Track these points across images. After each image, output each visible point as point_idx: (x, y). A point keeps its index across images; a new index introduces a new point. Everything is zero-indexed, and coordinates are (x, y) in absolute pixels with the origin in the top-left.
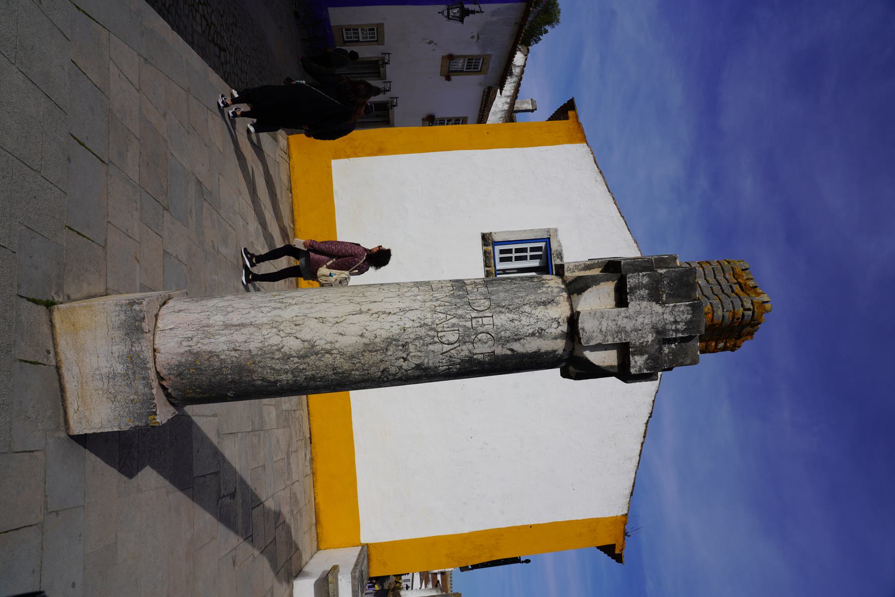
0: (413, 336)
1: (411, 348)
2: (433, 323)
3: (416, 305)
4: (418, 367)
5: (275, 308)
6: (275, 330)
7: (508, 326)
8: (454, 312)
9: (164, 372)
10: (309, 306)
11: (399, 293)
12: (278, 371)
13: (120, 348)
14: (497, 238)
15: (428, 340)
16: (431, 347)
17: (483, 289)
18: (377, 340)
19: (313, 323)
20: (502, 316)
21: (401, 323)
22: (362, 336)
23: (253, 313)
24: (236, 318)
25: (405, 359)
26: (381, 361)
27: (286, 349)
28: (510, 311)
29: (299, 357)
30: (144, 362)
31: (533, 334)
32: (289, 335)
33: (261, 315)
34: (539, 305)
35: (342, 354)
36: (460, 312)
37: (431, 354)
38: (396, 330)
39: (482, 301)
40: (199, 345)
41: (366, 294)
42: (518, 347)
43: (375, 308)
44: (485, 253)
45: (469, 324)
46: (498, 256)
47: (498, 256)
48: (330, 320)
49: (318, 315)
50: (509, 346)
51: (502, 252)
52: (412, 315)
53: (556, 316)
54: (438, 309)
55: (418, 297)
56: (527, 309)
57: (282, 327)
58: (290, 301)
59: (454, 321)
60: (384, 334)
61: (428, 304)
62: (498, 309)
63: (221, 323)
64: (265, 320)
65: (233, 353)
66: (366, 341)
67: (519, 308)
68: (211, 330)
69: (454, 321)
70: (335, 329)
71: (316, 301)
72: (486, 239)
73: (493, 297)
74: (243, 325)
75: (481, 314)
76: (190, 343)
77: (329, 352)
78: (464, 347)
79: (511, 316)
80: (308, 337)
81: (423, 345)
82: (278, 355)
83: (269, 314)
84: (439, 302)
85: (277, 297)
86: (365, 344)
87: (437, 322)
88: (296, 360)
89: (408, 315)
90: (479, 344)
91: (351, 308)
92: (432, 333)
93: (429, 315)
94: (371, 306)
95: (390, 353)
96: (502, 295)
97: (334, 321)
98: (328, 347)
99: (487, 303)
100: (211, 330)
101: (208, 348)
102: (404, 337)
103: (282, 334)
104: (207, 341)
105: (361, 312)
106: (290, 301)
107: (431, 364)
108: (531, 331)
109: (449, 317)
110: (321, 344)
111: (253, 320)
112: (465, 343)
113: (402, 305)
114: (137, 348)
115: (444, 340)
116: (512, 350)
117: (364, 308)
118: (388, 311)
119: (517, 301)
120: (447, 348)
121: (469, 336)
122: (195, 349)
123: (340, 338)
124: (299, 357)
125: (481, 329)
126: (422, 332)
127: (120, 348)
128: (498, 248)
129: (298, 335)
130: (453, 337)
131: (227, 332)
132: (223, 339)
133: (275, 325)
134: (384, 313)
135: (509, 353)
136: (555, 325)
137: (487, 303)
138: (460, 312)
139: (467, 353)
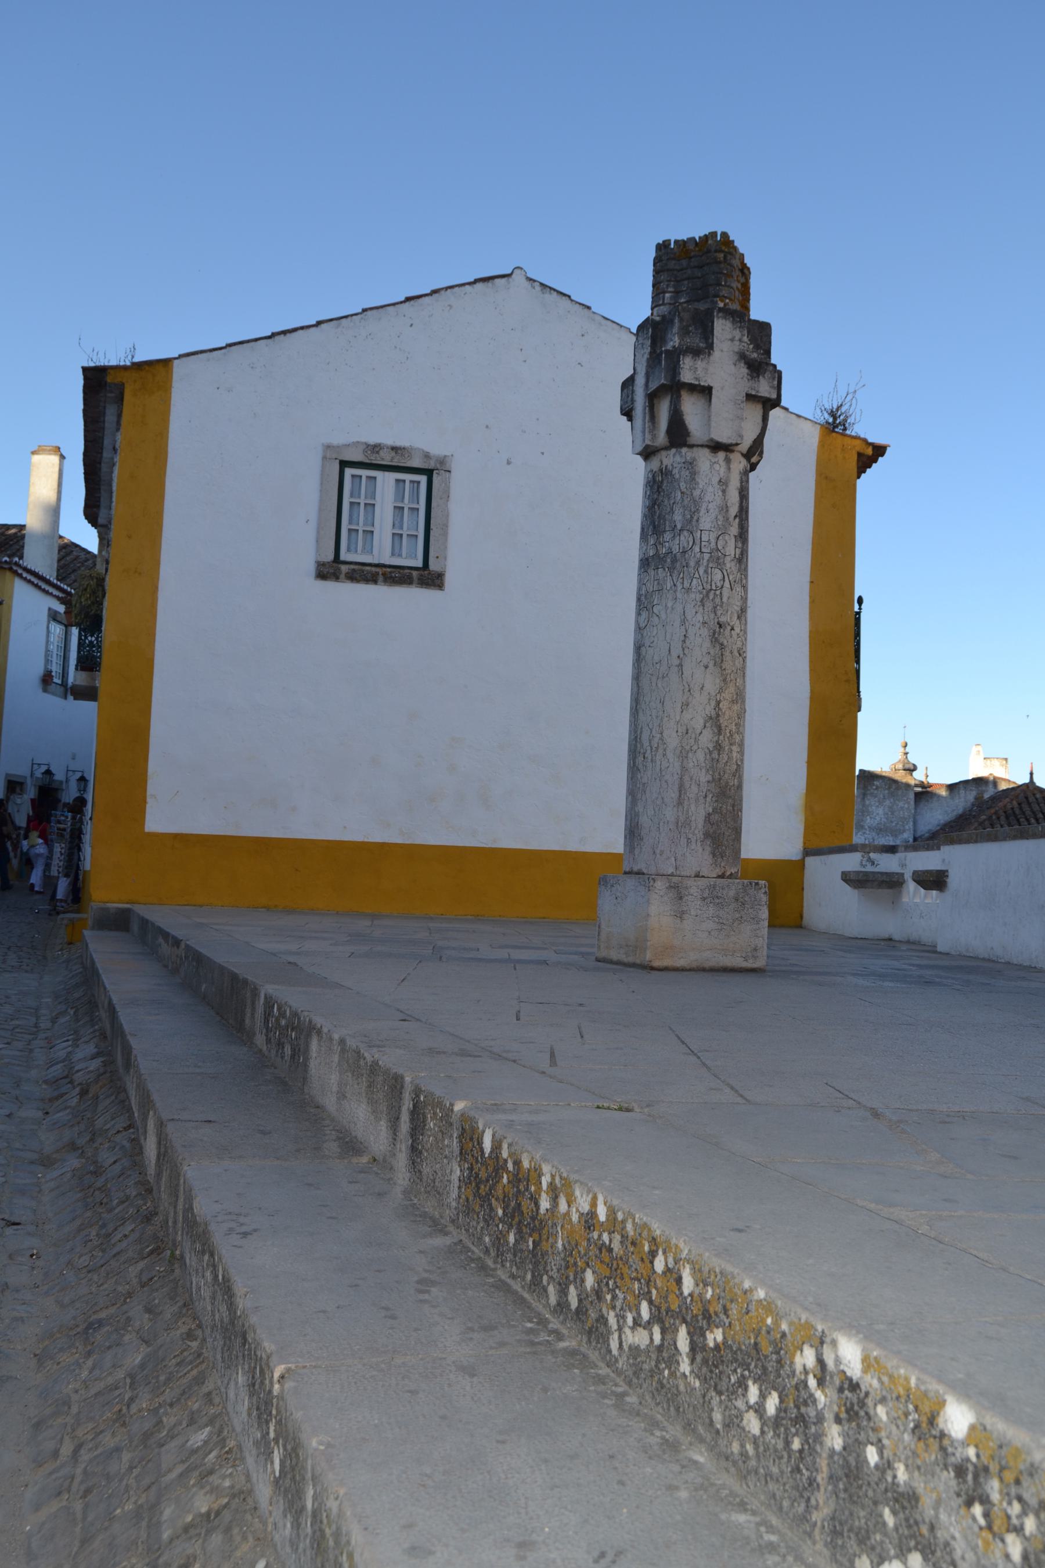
0: (712, 616)
1: (722, 619)
2: (701, 593)
3: (679, 608)
4: (739, 617)
5: (664, 755)
6: (690, 755)
7: (713, 516)
8: (692, 570)
9: (719, 871)
10: (666, 719)
11: (660, 627)
14: (330, 556)
15: (717, 600)
16: (725, 599)
17: (667, 536)
18: (712, 653)
19: (687, 716)
20: (702, 520)
21: (698, 625)
22: (706, 667)
23: (667, 777)
24: (672, 794)
25: (732, 629)
26: (731, 652)
27: (711, 746)
28: (698, 511)
29: (720, 733)
31: (724, 491)
32: (696, 740)
33: (670, 769)
34: (694, 479)
35: (721, 691)
36: (692, 564)
37: (731, 600)
38: (705, 632)
39: (682, 538)
40: (696, 832)
41: (656, 659)
42: (734, 510)
43: (676, 651)
44: (352, 577)
45: (707, 556)
48: (685, 697)
49: (679, 710)
50: (731, 519)
52: (690, 613)
53: (708, 463)
54: (686, 585)
55: (670, 604)
56: (697, 493)
57: (688, 748)
58: (656, 740)
59: (701, 570)
60: (707, 644)
61: (679, 595)
62: (694, 523)
63: (675, 809)
64: (677, 764)
65: (708, 799)
66: (711, 665)
67: (695, 501)
68: (682, 819)
69: (701, 570)
71: (661, 713)
72: (329, 571)
73: (679, 527)
74: (681, 788)
75: (698, 542)
76: (693, 840)
77: (718, 703)
78: (728, 565)
79: (703, 511)
80: (702, 722)
81: (721, 606)
82: (715, 755)
83: (671, 760)
84: (678, 584)
85: (648, 755)
86: (715, 665)
87: (700, 588)
88: (721, 737)
89: (689, 617)
90: (727, 549)
91: (674, 676)
92: (711, 596)
93: (693, 596)
94: (674, 654)
95: (725, 643)
97: (687, 694)
98: (713, 703)
99: (685, 533)
100: (682, 819)
102: (713, 624)
103: (695, 748)
104: (693, 824)
105: (681, 665)
106: (656, 740)
107: (739, 604)
108: (720, 493)
109: (697, 575)
110: (710, 710)
111: (676, 777)
112: (724, 564)
113: (677, 623)
115: (719, 584)
116: (736, 517)
117: (677, 662)
118: (682, 638)
119: (686, 502)
120: (727, 584)
121: (718, 558)
122: (700, 835)
124: (720, 732)
126: (709, 605)
128: (344, 556)
129: (698, 732)
130: (718, 576)
131: (686, 803)
132: (693, 807)
133: (683, 755)
134: (684, 641)
135: (737, 520)
136: (717, 467)
137: (685, 533)
138: (692, 564)
139: (733, 564)
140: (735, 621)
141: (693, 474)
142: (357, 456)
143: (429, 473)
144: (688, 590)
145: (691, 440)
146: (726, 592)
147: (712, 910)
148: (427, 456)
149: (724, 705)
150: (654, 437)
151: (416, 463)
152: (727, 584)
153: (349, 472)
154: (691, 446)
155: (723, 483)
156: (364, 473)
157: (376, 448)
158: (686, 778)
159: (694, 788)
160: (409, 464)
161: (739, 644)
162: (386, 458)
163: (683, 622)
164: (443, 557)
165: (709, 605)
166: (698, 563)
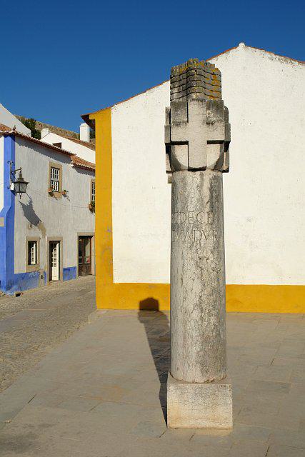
15: (198, 246)
16: (202, 245)
19: (185, 304)
25: (208, 259)
27: (197, 318)
31: (200, 191)
35: (202, 291)
36: (185, 229)
42: (206, 200)
45: (192, 225)
52: (185, 253)
53: (191, 178)
60: (194, 268)
70: (189, 293)
82: (200, 323)
88: (203, 314)
98: (198, 298)
101: (194, 355)
102: (196, 258)
110: (196, 300)
123: (194, 291)
125: (195, 218)
130: (198, 234)
136: (196, 179)
144: (184, 242)
146: (203, 241)
147: (201, 400)
155: (200, 187)
165: (194, 249)
166: (188, 229)
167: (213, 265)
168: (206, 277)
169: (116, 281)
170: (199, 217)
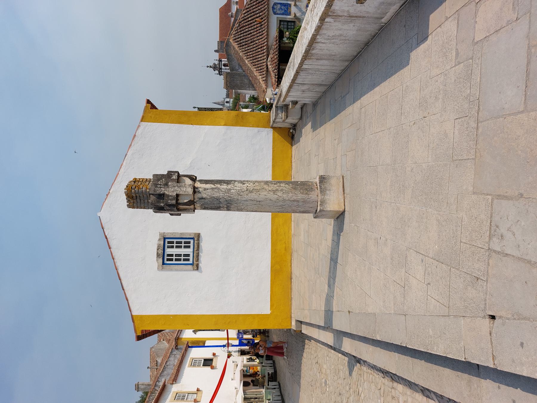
1: (245, 189)
3: (243, 202)
4: (244, 184)
9: (316, 190)
12: (285, 187)
13: (327, 197)
14: (190, 267)
17: (221, 205)
30: (321, 193)
38: (250, 195)
42: (213, 186)
44: (198, 260)
46: (191, 258)
47: (191, 258)
51: (188, 260)
56: (208, 197)
60: (253, 194)
70: (267, 197)
82: (284, 191)
96: (215, 203)
102: (247, 192)
105: (259, 201)
114: (323, 197)
120: (235, 188)
127: (327, 197)
128: (191, 262)
140: (245, 185)
141: (202, 198)
142: (161, 260)
143: (165, 239)
145: (192, 199)
146: (238, 189)
148: (159, 240)
149: (270, 189)
150: (191, 209)
151: (162, 243)
152: (235, 188)
153: (166, 262)
154: (194, 199)
155: (205, 189)
156: (166, 257)
157: (158, 255)
158: (291, 199)
159: (294, 197)
160: (162, 245)
161: (252, 184)
162: (161, 252)
163: (247, 201)
164: (190, 234)
165: (242, 194)
166: (229, 197)
167: (252, 184)
168: (259, 188)
169: (268, 312)
170: (223, 190)
